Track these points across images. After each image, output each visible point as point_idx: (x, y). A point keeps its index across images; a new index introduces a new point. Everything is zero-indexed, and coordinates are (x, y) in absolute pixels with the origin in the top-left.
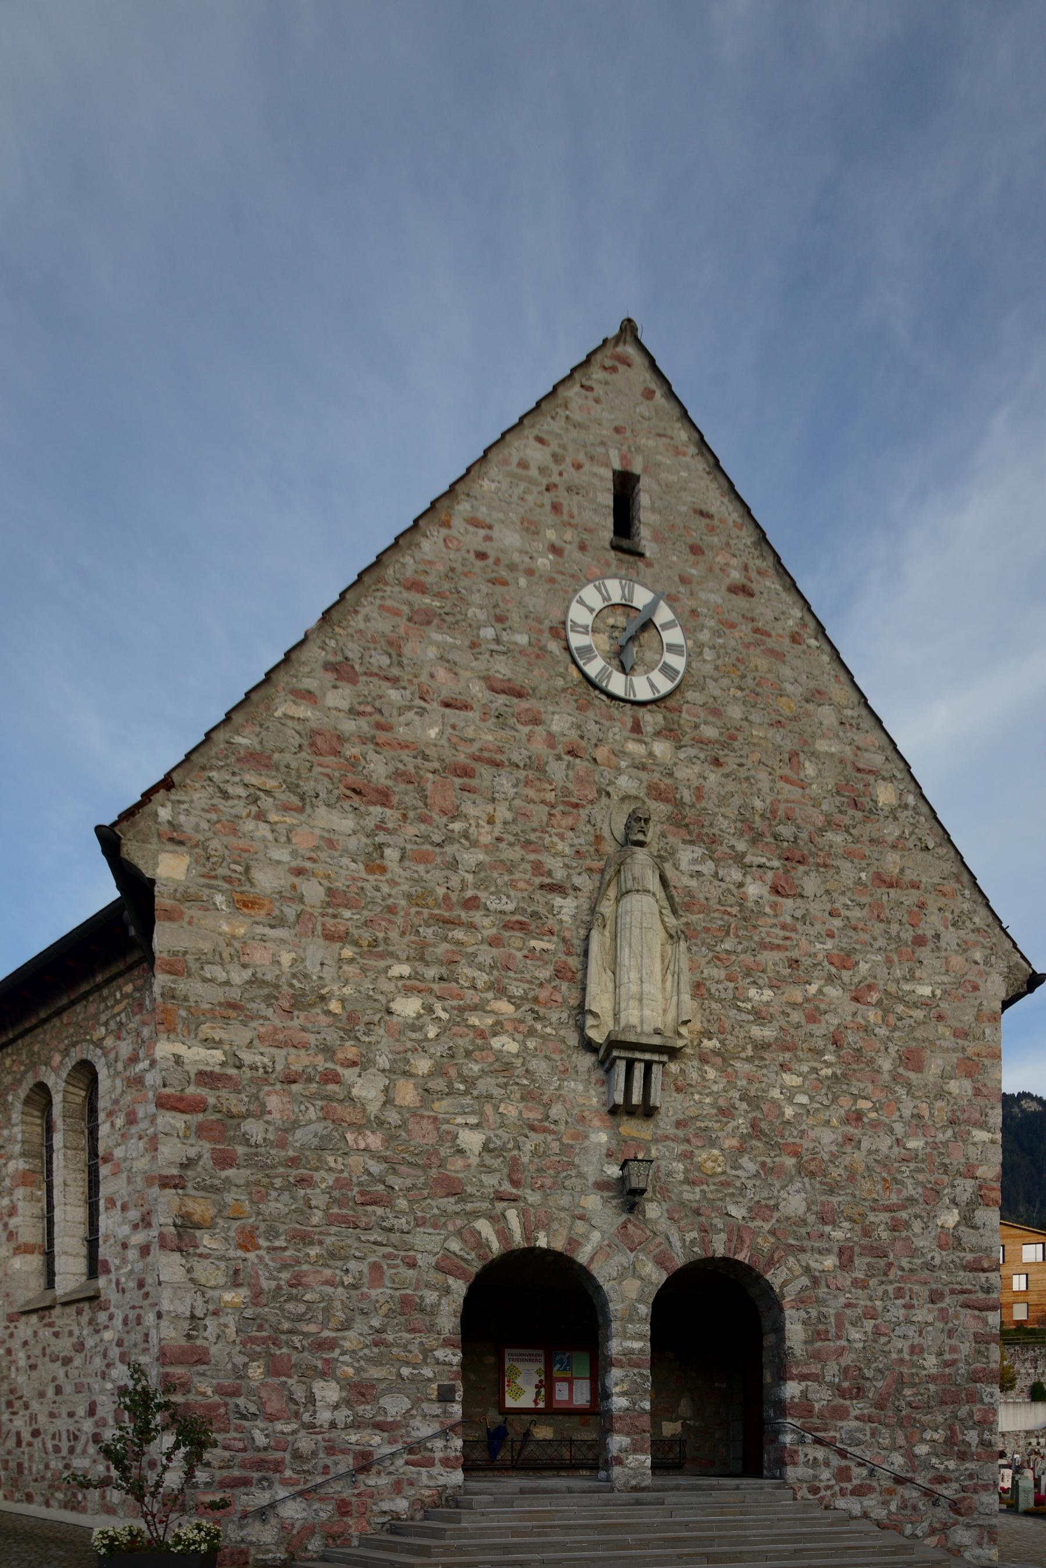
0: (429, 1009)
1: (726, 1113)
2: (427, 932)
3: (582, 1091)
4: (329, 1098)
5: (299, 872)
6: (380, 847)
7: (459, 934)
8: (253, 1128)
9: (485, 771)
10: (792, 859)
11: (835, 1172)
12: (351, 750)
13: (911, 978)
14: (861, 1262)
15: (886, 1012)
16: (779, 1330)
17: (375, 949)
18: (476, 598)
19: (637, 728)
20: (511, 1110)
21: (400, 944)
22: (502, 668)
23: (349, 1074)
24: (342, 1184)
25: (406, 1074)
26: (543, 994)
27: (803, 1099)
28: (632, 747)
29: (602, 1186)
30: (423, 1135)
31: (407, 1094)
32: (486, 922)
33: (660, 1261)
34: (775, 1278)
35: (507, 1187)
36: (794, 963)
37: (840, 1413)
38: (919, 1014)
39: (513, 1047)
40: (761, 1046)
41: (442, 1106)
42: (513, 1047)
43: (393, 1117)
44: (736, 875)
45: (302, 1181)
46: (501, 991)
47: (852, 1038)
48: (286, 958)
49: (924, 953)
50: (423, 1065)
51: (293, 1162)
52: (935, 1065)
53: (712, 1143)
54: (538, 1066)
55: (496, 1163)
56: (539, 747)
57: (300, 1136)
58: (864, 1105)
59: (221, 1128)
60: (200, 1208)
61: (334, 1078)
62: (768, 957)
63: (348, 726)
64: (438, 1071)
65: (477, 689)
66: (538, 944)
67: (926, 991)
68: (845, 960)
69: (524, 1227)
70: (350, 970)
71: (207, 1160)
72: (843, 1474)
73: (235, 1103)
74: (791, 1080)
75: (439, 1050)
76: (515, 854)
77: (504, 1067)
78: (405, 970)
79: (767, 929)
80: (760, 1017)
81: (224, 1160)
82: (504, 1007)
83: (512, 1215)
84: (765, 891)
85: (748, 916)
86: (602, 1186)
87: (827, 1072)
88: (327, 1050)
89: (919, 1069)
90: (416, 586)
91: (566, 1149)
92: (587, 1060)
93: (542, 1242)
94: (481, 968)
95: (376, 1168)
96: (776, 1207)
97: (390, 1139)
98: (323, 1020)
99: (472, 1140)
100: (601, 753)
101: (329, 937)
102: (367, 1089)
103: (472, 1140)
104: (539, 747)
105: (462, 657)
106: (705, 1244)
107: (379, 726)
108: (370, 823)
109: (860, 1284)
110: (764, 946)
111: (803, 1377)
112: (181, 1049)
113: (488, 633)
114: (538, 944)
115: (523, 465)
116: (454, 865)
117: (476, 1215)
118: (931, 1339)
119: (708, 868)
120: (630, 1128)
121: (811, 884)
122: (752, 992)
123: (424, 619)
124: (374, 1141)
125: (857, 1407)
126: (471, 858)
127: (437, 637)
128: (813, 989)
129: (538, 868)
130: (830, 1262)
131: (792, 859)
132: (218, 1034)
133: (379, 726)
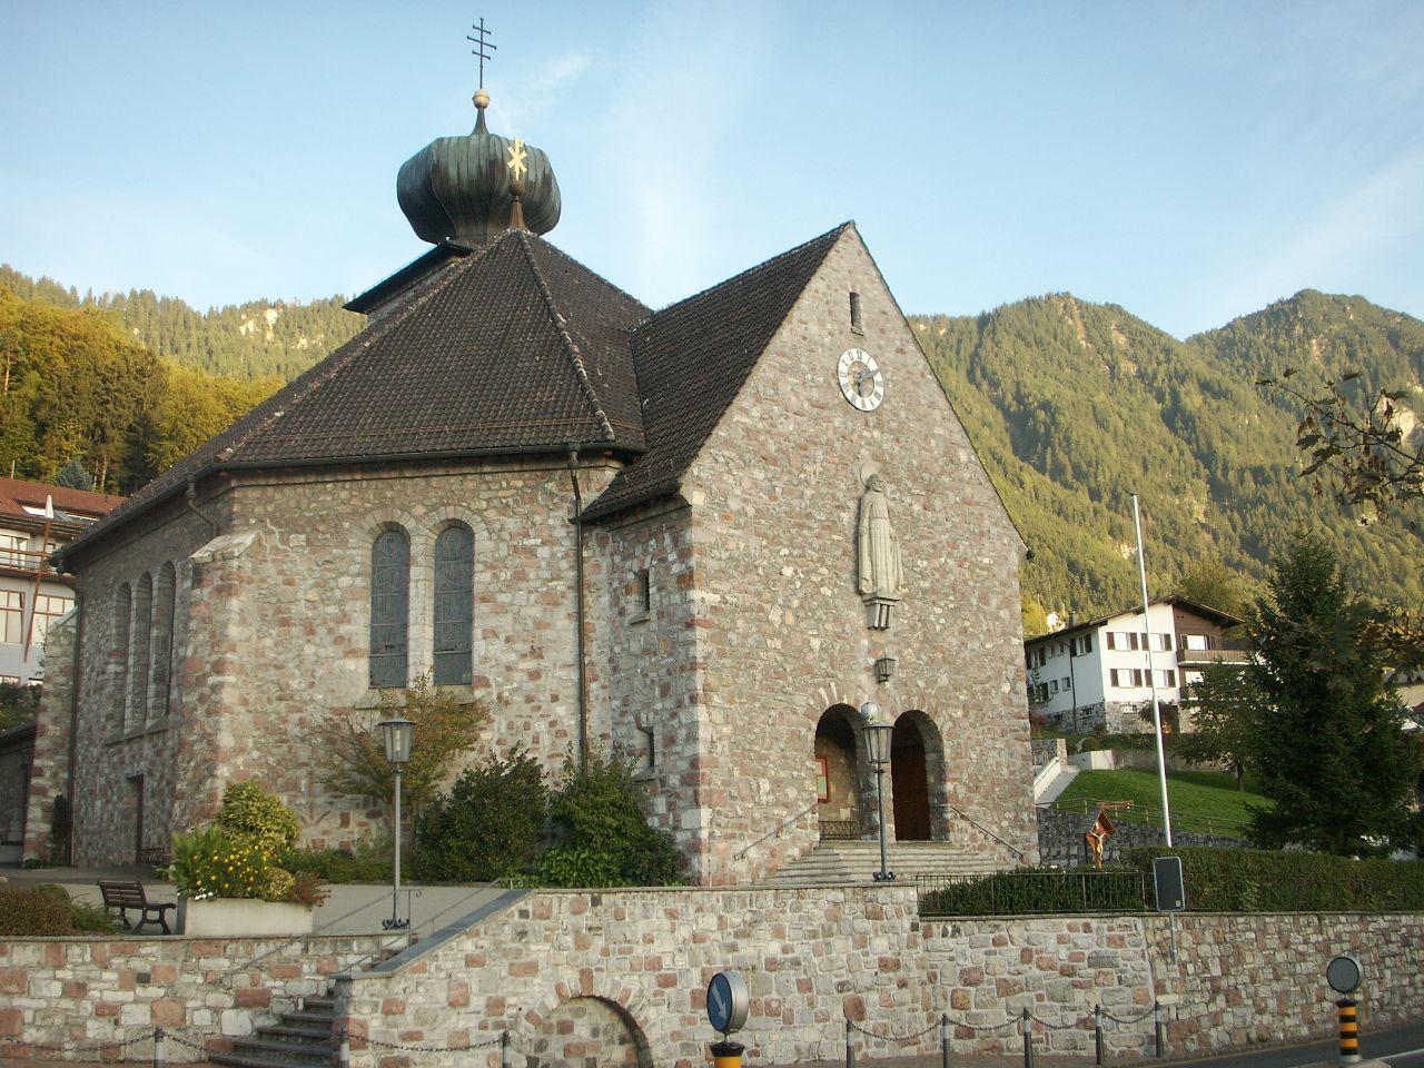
0: (796, 571)
1: (913, 628)
2: (793, 531)
3: (856, 616)
4: (759, 620)
5: (745, 500)
6: (774, 487)
7: (805, 532)
8: (732, 636)
9: (812, 448)
10: (930, 490)
11: (959, 661)
12: (762, 438)
13: (980, 554)
14: (972, 713)
15: (972, 572)
16: (939, 751)
17: (774, 541)
18: (803, 359)
19: (867, 424)
20: (829, 626)
21: (784, 538)
22: (815, 394)
23: (767, 606)
24: (767, 668)
25: (789, 607)
26: (839, 564)
27: (942, 621)
28: (865, 433)
29: (867, 669)
30: (797, 641)
31: (790, 620)
32: (815, 525)
33: (892, 713)
34: (939, 722)
35: (830, 670)
36: (934, 546)
37: (970, 801)
38: (985, 573)
39: (829, 593)
40: (925, 592)
41: (803, 625)
42: (829, 593)
43: (785, 632)
44: (909, 500)
45: (752, 666)
46: (823, 564)
47: (961, 588)
48: (742, 546)
49: (985, 539)
50: (796, 603)
51: (747, 656)
52: (994, 602)
53: (909, 645)
54: (839, 602)
55: (825, 656)
56: (830, 434)
57: (750, 641)
58: (967, 624)
59: (720, 636)
60: (712, 680)
61: (761, 609)
62: (924, 543)
63: (760, 426)
64: (801, 606)
65: (806, 405)
66: (835, 537)
67: (986, 561)
68: (954, 545)
69: (838, 691)
70: (766, 551)
71: (714, 655)
72: (973, 838)
73: (725, 622)
74: (938, 611)
75: (800, 595)
76: (824, 490)
77: (825, 603)
78: (785, 551)
79: (923, 529)
80: (924, 577)
81: (722, 654)
82: (824, 570)
83: (833, 684)
84: (921, 508)
85: (915, 521)
86: (867, 669)
87: (951, 606)
88: (758, 594)
89: (987, 604)
90: (782, 354)
91: (852, 648)
92: (858, 600)
93: (845, 702)
94: (814, 550)
95: (779, 658)
96: (936, 682)
97: (784, 642)
98: (756, 578)
99: (815, 643)
100: (855, 437)
101: (758, 535)
102: (775, 617)
103: (815, 643)
104: (830, 434)
105: (800, 389)
106: (910, 703)
107: (772, 425)
108: (770, 475)
109: (973, 725)
110: (923, 537)
111: (954, 780)
112: (704, 594)
113: (809, 377)
114: (835, 537)
115: (817, 291)
116: (802, 496)
117: (817, 685)
118: (1004, 759)
119: (897, 496)
120: (877, 636)
121: (938, 504)
122: (919, 562)
123: (784, 370)
124: (778, 643)
125: (977, 798)
126: (809, 492)
127: (790, 380)
128: (942, 560)
129: (834, 498)
130: (960, 713)
131: (930, 490)
132: (718, 586)
133: (772, 425)
